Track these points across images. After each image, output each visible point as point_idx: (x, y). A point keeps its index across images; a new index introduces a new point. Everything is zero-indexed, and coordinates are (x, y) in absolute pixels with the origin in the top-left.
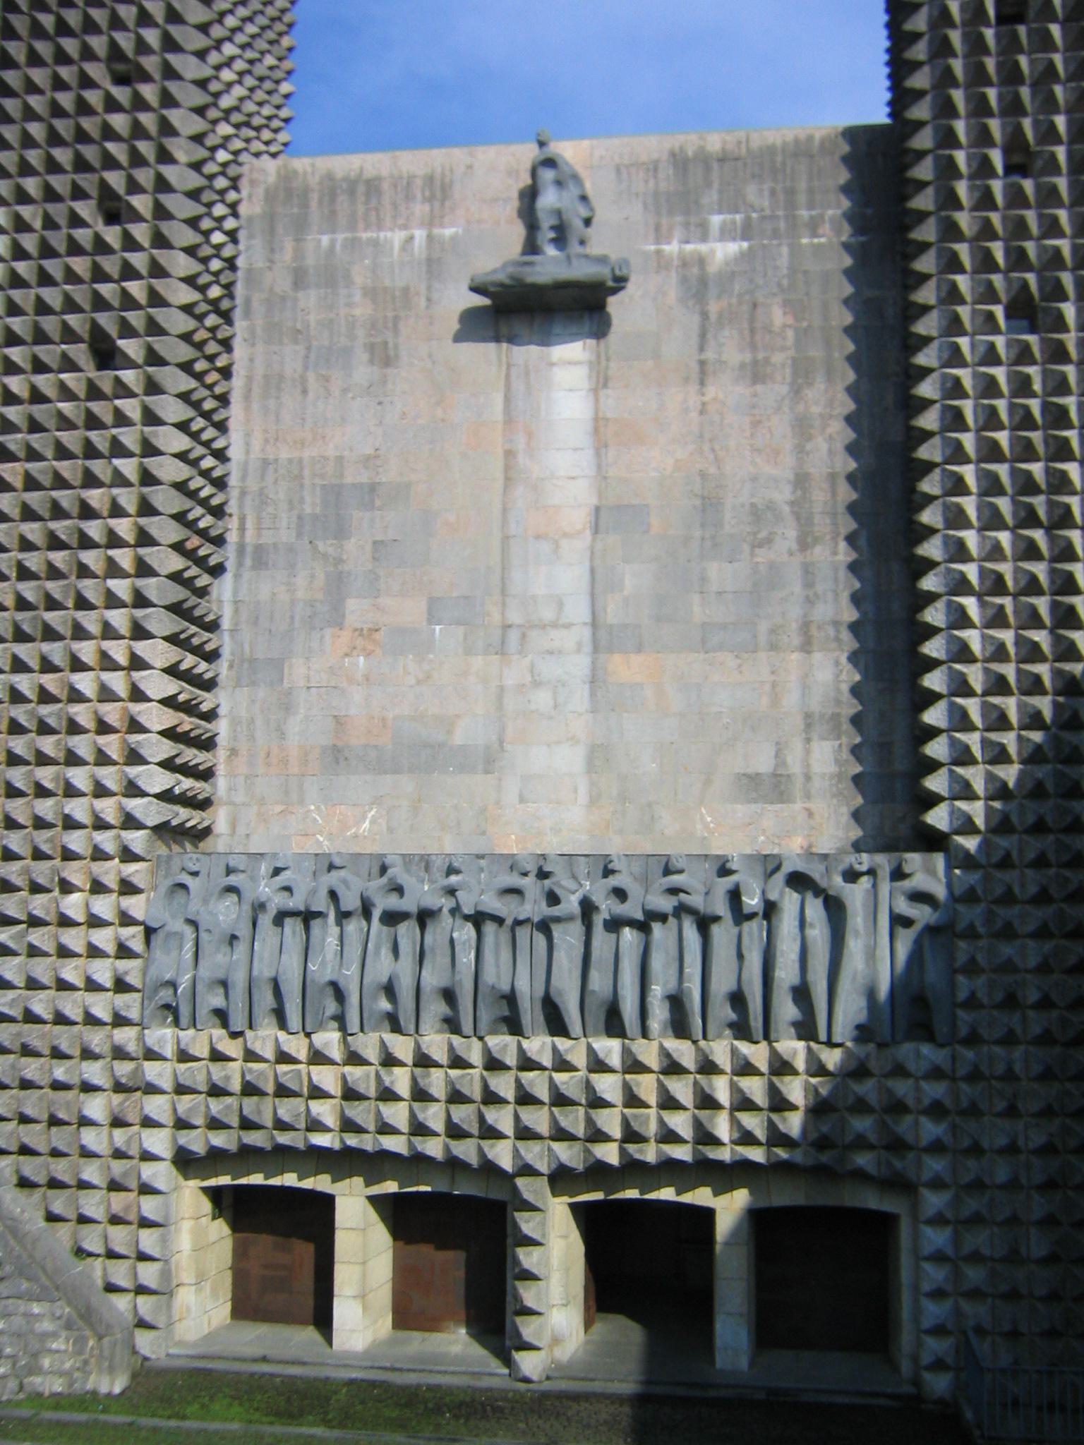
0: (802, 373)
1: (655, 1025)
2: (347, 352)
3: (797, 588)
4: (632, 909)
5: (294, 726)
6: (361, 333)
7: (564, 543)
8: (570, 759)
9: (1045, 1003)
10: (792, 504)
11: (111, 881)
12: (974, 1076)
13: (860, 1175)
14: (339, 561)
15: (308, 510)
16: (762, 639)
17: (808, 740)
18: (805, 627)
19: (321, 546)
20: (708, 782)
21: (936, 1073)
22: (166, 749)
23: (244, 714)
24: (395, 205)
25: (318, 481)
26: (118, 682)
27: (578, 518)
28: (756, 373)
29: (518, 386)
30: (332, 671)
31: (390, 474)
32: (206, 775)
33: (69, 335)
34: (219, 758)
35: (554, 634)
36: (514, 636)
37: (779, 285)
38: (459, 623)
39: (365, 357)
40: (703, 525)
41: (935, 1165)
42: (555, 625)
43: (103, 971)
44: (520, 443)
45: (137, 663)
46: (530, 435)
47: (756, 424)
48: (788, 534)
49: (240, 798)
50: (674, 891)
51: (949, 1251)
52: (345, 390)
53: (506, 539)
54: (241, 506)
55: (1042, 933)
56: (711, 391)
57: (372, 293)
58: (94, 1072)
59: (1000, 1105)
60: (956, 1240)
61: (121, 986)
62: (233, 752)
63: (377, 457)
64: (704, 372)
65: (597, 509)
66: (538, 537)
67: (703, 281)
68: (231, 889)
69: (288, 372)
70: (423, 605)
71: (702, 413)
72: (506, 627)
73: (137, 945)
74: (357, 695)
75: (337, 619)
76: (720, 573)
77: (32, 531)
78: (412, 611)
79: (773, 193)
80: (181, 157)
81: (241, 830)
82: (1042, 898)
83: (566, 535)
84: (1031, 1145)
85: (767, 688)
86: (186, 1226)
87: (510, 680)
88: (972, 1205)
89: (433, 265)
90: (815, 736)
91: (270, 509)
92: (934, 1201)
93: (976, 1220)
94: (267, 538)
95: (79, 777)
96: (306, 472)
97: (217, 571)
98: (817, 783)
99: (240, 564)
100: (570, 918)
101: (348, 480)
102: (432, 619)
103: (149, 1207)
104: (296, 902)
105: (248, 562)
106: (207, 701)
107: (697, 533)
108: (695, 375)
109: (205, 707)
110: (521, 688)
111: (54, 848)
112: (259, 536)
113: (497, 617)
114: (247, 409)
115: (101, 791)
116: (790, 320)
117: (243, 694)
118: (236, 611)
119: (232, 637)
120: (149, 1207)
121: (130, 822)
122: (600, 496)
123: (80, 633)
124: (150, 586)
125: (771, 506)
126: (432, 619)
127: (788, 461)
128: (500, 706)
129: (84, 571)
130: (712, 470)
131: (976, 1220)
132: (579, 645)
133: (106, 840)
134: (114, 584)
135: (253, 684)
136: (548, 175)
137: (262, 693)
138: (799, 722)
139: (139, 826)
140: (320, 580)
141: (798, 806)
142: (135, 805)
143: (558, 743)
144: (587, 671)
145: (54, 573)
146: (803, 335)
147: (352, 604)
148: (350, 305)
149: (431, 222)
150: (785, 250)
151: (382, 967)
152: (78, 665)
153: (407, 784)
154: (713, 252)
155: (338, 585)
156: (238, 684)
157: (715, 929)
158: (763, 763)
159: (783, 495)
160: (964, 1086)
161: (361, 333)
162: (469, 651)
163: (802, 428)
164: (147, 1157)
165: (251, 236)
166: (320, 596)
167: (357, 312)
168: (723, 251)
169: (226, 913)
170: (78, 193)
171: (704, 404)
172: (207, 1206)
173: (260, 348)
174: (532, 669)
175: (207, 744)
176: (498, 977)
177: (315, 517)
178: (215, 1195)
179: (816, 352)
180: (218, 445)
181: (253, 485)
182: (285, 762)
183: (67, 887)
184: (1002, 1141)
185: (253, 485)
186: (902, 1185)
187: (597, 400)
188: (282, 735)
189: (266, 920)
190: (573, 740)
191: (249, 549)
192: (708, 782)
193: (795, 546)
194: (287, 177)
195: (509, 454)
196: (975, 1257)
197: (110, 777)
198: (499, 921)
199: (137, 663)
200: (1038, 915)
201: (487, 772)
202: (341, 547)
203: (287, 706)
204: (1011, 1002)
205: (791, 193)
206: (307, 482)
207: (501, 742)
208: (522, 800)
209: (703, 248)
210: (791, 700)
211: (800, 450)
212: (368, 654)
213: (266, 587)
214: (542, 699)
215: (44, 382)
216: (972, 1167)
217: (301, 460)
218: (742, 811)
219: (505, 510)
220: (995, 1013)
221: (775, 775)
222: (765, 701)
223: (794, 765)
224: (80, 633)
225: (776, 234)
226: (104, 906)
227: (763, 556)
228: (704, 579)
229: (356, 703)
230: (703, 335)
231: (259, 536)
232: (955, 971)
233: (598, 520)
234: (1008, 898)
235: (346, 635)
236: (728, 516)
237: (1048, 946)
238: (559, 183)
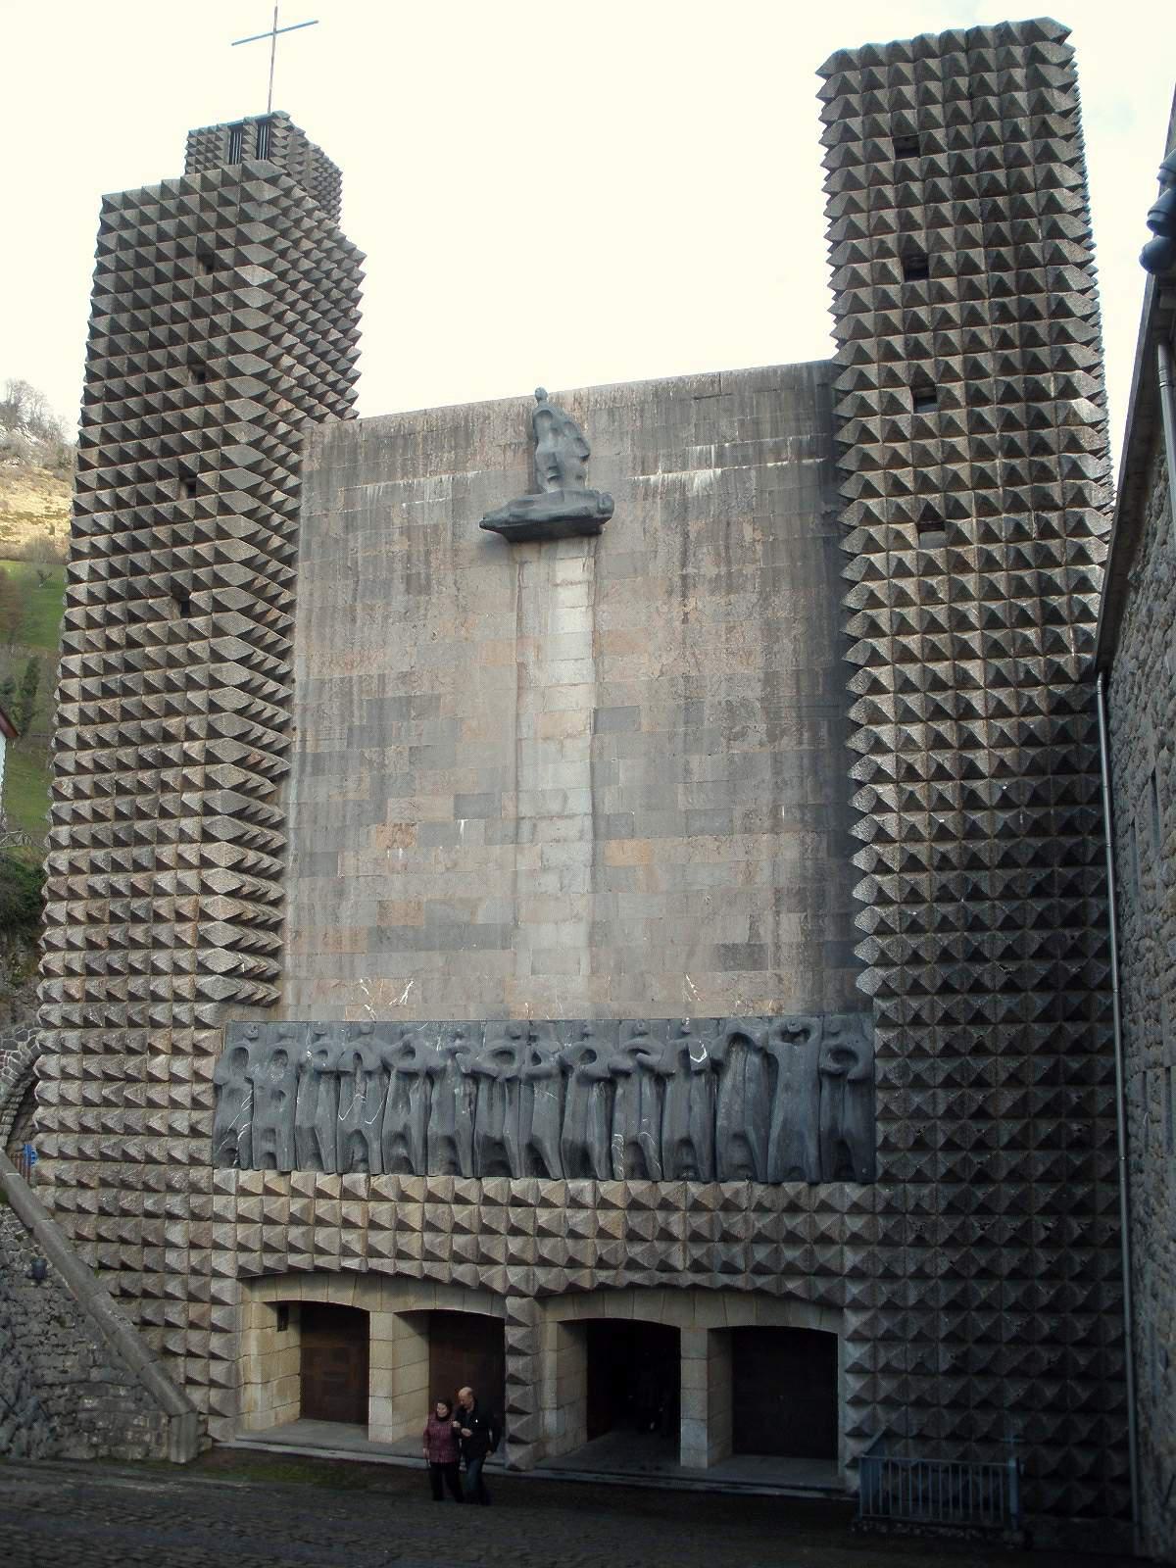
0: (770, 581)
1: (620, 1169)
2: (387, 584)
3: (768, 775)
4: (596, 1068)
5: (346, 910)
6: (398, 566)
7: (568, 742)
8: (572, 935)
9: (950, 1146)
10: (762, 700)
11: (185, 1045)
12: (889, 1210)
13: (790, 1297)
14: (383, 766)
15: (357, 723)
16: (738, 823)
17: (778, 913)
18: (775, 811)
20: (691, 954)
21: (856, 1209)
22: (232, 933)
23: (306, 900)
24: (427, 456)
25: (365, 697)
26: (190, 878)
27: (580, 720)
28: (729, 584)
29: (528, 606)
31: (423, 689)
32: (275, 953)
33: (155, 591)
34: (285, 940)
35: (560, 823)
36: (526, 827)
37: (749, 505)
38: (480, 817)
39: (402, 587)
40: (686, 723)
41: (854, 1290)
42: (560, 817)
43: (181, 1121)
44: (531, 657)
45: (206, 863)
46: (539, 648)
47: (730, 630)
49: (303, 974)
50: (635, 1051)
51: (868, 1365)
52: (386, 618)
53: (519, 741)
54: (303, 722)
55: (949, 1083)
56: (692, 603)
57: (407, 531)
58: (174, 1203)
59: (911, 1237)
60: (874, 1357)
61: (195, 1132)
62: (298, 933)
63: (411, 674)
64: (686, 584)
65: (596, 711)
66: (546, 739)
67: (685, 505)
68: (281, 1053)
69: (340, 603)
70: (451, 802)
71: (685, 621)
72: (519, 819)
73: (207, 1100)
74: (397, 882)
76: (702, 765)
77: (126, 755)
78: (441, 808)
79: (742, 423)
80: (243, 438)
81: (305, 1001)
82: (949, 1051)
83: (569, 736)
84: (940, 1272)
85: (743, 865)
86: (254, 1334)
87: (522, 867)
88: (885, 1324)
89: (457, 506)
90: (784, 908)
91: (326, 723)
92: (854, 1321)
93: (889, 1338)
94: (323, 748)
95: (161, 959)
96: (355, 689)
97: (279, 778)
98: (785, 953)
99: (302, 771)
100: (548, 1076)
101: (390, 694)
103: (217, 1315)
104: (325, 1063)
105: (309, 769)
106: (274, 890)
107: (681, 730)
108: (678, 589)
109: (272, 896)
110: (532, 874)
111: (143, 1018)
112: (317, 746)
113: (511, 809)
114: (308, 636)
115: (179, 971)
116: (758, 535)
117: (304, 884)
118: (299, 813)
119: (297, 835)
120: (217, 1315)
121: (201, 996)
122: (599, 697)
123: (162, 839)
124: (216, 799)
125: (745, 703)
126: (458, 815)
127: (759, 660)
129: (164, 786)
131: (889, 1338)
132: (582, 832)
133: (182, 1012)
134: (187, 797)
135: (313, 874)
136: (545, 424)
137: (321, 881)
138: (770, 896)
139: (210, 1000)
141: (769, 973)
142: (205, 982)
143: (564, 921)
144: (589, 856)
145: (143, 789)
146: (771, 548)
148: (389, 542)
149: (455, 466)
150: (753, 473)
151: (396, 1121)
152: (161, 866)
153: (438, 959)
154: (692, 480)
155: (381, 786)
156: (301, 875)
157: (670, 1087)
158: (739, 935)
159: (754, 693)
160: (881, 1221)
161: (398, 566)
162: (489, 841)
163: (770, 630)
164: (217, 1274)
165: (311, 489)
166: (367, 797)
167: (396, 548)
168: (701, 477)
169: (277, 1075)
170: (163, 474)
171: (686, 614)
172: (272, 1317)
173: (318, 584)
175: (276, 927)
176: (491, 1127)
177: (362, 728)
178: (283, 1310)
179: (783, 563)
180: (283, 669)
181: (312, 702)
182: (339, 942)
183: (155, 1051)
184: (912, 1268)
185: (312, 702)
186: (830, 1306)
187: (595, 615)
188: (337, 919)
189: (305, 1079)
190: (577, 918)
191: (309, 758)
192: (691, 954)
193: (765, 739)
194: (340, 435)
195: (522, 666)
196: (888, 1370)
197: (184, 958)
198: (492, 1079)
199: (206, 863)
200: (946, 1067)
201: (503, 948)
202: (383, 753)
203: (340, 893)
204: (920, 1145)
205: (757, 423)
206: (355, 697)
207: (516, 920)
208: (534, 972)
209: (683, 475)
210: (763, 877)
211: (768, 651)
212: (406, 847)
213: (324, 790)
214: (550, 882)
215: (134, 630)
216: (885, 1290)
217: (351, 678)
218: (721, 978)
219: (518, 716)
220: (909, 1155)
221: (749, 945)
222: (741, 877)
223: (767, 939)
224: (162, 839)
225: (745, 460)
226: (181, 1067)
228: (687, 771)
229: (396, 889)
230: (685, 553)
231: (317, 746)
232: (876, 1119)
234: (919, 1052)
235: (389, 829)
236: (707, 712)
237: (953, 1095)
238: (556, 431)
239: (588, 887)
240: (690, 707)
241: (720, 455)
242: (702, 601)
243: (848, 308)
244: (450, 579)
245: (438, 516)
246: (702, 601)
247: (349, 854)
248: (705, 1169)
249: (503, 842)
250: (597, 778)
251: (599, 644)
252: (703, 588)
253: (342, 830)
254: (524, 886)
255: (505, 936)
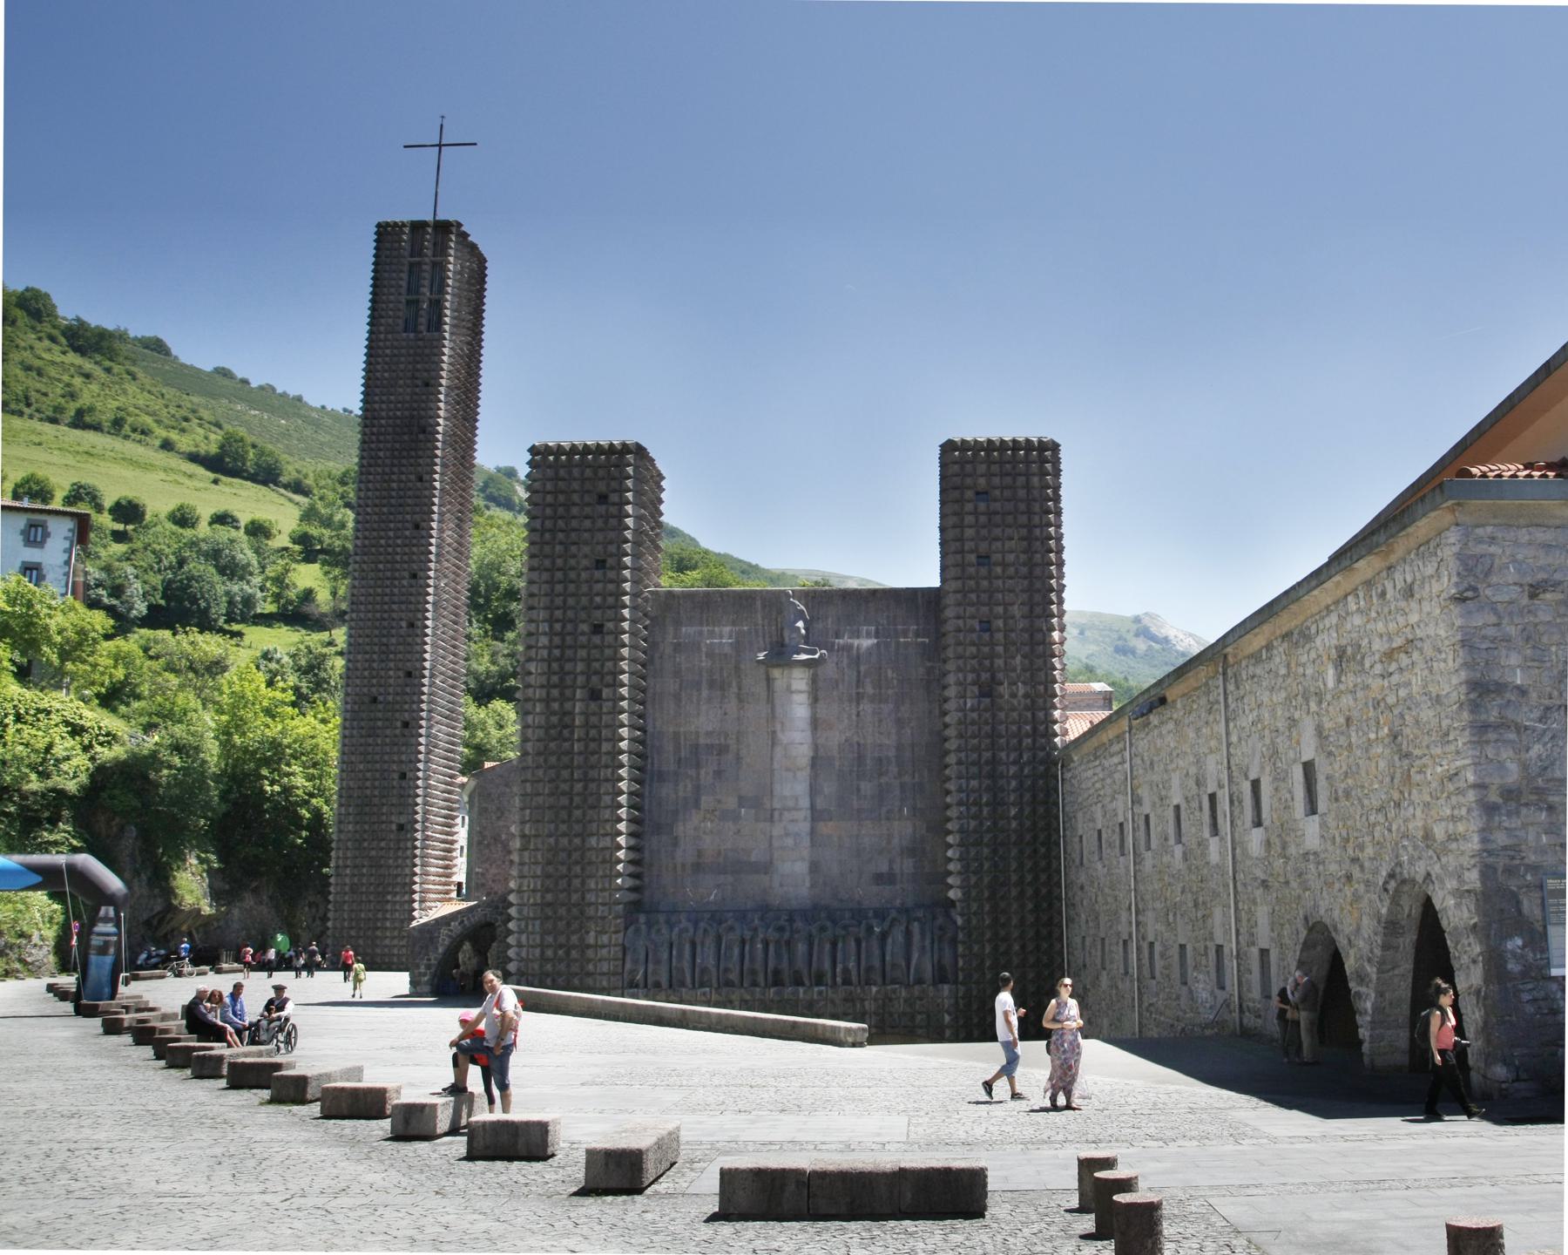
1: (839, 980)
5: (679, 853)
7: (799, 774)
15: (683, 755)
19: (689, 772)
28: (879, 699)
30: (696, 829)
36: (776, 814)
44: (778, 727)
46: (782, 723)
47: (880, 721)
48: (894, 769)
57: (710, 655)
64: (859, 698)
66: (788, 770)
71: (858, 715)
72: (773, 810)
74: (708, 839)
75: (697, 804)
78: (731, 802)
79: (888, 617)
87: (775, 833)
102: (741, 805)
126: (741, 805)
128: (771, 845)
130: (862, 742)
140: (690, 786)
147: (703, 798)
153: (730, 879)
155: (698, 789)
158: (884, 868)
159: (892, 753)
161: (705, 674)
162: (757, 820)
163: (899, 722)
168: (866, 643)
174: (785, 828)
182: (675, 867)
188: (673, 858)
190: (803, 859)
195: (774, 732)
201: (766, 873)
203: (675, 842)
210: (896, 841)
212: (712, 821)
214: (790, 841)
227: (884, 780)
228: (858, 790)
229: (708, 843)
230: (858, 681)
233: (815, 762)
239: (808, 844)
240: (860, 758)
241: (877, 632)
242: (866, 707)
243: (943, 569)
244: (734, 684)
245: (727, 650)
246: (866, 707)
247: (680, 824)
248: (879, 980)
249: (765, 821)
250: (814, 791)
251: (815, 723)
252: (865, 701)
253: (676, 812)
254: (776, 844)
255: (766, 867)
